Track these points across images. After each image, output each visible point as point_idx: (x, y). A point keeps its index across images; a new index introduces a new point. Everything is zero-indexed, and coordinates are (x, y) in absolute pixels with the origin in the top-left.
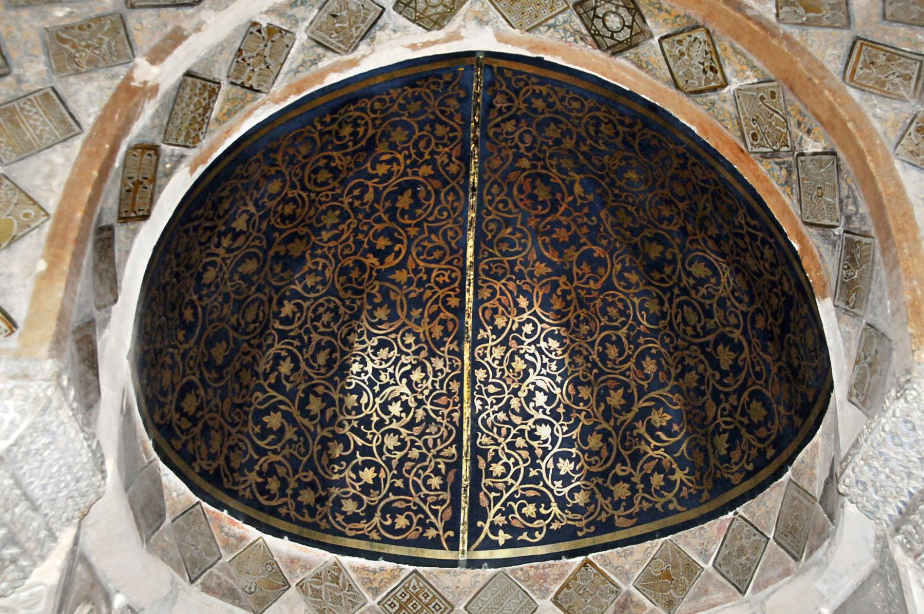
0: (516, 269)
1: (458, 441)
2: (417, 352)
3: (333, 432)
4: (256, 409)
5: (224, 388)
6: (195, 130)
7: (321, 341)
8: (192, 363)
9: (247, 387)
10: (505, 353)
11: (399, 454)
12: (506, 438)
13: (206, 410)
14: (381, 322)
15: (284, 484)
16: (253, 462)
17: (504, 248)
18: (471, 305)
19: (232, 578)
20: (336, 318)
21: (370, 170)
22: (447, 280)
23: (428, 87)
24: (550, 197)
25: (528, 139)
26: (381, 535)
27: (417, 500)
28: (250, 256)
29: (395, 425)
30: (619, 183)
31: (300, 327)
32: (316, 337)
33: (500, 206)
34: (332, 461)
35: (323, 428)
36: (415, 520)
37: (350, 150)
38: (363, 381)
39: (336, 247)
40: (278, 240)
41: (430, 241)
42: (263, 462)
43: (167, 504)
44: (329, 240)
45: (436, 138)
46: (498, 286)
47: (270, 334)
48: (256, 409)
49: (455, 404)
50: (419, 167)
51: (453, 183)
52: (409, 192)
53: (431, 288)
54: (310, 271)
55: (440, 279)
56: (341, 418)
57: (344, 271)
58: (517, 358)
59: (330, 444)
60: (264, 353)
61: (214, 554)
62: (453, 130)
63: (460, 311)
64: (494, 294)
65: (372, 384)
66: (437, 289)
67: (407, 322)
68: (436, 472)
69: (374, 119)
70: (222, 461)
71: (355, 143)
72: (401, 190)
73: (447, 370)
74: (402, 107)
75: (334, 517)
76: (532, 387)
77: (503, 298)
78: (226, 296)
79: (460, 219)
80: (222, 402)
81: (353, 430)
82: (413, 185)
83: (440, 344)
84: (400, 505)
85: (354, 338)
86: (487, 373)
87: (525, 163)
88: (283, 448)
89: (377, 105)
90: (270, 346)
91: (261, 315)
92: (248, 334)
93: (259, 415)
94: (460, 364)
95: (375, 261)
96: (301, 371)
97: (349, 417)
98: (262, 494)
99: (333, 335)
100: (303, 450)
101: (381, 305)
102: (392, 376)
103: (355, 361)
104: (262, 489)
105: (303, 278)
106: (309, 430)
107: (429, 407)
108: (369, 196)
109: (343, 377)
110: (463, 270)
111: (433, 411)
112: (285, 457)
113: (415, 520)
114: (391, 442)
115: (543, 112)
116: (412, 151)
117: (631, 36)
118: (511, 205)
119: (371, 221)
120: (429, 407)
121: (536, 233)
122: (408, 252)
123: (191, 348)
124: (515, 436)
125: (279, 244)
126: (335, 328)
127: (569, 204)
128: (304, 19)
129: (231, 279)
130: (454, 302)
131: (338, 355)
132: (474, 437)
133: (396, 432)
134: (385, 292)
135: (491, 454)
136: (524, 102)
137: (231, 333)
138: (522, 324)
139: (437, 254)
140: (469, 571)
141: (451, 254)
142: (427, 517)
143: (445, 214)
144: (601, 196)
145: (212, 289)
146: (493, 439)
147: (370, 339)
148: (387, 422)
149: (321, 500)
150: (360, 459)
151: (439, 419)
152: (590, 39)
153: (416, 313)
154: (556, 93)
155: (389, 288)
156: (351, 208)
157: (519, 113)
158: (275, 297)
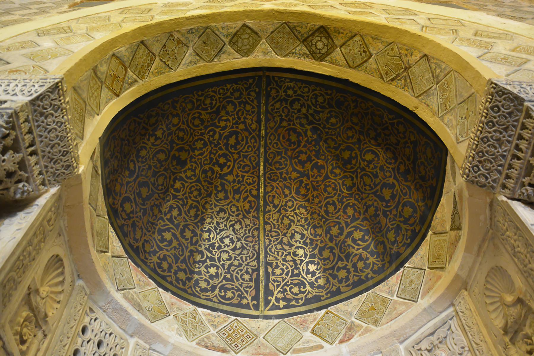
0: (283, 176)
4: (159, 228)
5: (145, 210)
7: (192, 204)
8: (131, 189)
9: (156, 216)
10: (280, 216)
13: (135, 216)
14: (221, 200)
17: (277, 166)
18: (263, 195)
20: (200, 194)
21: (217, 124)
22: (252, 182)
23: (243, 85)
24: (297, 139)
25: (286, 110)
28: (163, 151)
30: (327, 126)
31: (183, 195)
32: (190, 202)
33: (275, 145)
35: (191, 245)
37: (209, 111)
38: (211, 227)
39: (201, 159)
40: (175, 149)
41: (244, 162)
42: (161, 254)
43: (110, 246)
44: (199, 155)
45: (247, 111)
46: (275, 184)
47: (169, 195)
48: (159, 228)
49: (256, 242)
50: (239, 124)
51: (254, 134)
52: (234, 137)
53: (244, 185)
54: (189, 169)
55: (248, 181)
56: (200, 242)
57: (205, 172)
58: (285, 218)
59: (194, 254)
60: (165, 203)
61: (132, 284)
62: (253, 108)
63: (257, 197)
64: (273, 189)
65: (216, 229)
66: (247, 185)
67: (233, 200)
69: (220, 98)
70: (140, 244)
71: (212, 108)
72: (231, 134)
73: (252, 225)
74: (232, 94)
77: (278, 190)
78: (150, 167)
79: (257, 152)
80: (144, 216)
82: (236, 133)
83: (248, 212)
85: (207, 206)
86: (271, 227)
87: (284, 124)
89: (221, 91)
90: (169, 201)
91: (165, 185)
92: (158, 190)
93: (160, 232)
94: (258, 222)
96: (182, 216)
99: (198, 202)
100: (181, 253)
101: (221, 191)
102: (226, 226)
103: (208, 218)
105: (185, 172)
106: (184, 244)
107: (243, 242)
108: (217, 136)
110: (259, 177)
111: (245, 244)
112: (172, 254)
115: (292, 97)
116: (236, 116)
117: (328, 49)
118: (279, 145)
119: (217, 149)
120: (243, 242)
121: (291, 158)
122: (234, 166)
125: (176, 150)
126: (199, 199)
127: (306, 142)
129: (153, 159)
130: (255, 192)
131: (200, 213)
134: (222, 185)
136: (284, 92)
137: (151, 186)
138: (287, 202)
139: (247, 169)
141: (253, 169)
143: (250, 148)
144: (320, 134)
147: (215, 207)
148: (223, 247)
152: (310, 56)
153: (237, 197)
154: (297, 85)
155: (224, 184)
156: (209, 141)
157: (282, 98)
158: (172, 177)
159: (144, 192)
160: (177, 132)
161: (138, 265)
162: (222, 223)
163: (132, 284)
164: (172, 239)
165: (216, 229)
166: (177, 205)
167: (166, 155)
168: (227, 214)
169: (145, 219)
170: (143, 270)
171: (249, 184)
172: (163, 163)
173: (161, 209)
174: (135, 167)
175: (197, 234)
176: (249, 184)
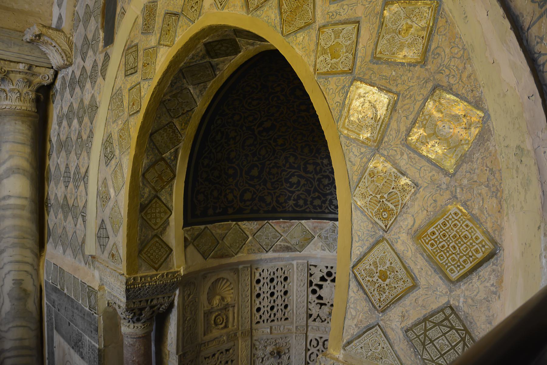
3: (322, 175)
15: (305, 201)
19: (288, 242)
35: (317, 175)
43: (248, 233)
59: (322, 180)
88: (301, 188)
93: (287, 181)
98: (296, 207)
100: (310, 186)
106: (311, 178)
112: (303, 191)
128: (183, 84)
149: (324, 202)
159: (255, 172)
161: (278, 218)
169: (269, 185)
170: (284, 219)
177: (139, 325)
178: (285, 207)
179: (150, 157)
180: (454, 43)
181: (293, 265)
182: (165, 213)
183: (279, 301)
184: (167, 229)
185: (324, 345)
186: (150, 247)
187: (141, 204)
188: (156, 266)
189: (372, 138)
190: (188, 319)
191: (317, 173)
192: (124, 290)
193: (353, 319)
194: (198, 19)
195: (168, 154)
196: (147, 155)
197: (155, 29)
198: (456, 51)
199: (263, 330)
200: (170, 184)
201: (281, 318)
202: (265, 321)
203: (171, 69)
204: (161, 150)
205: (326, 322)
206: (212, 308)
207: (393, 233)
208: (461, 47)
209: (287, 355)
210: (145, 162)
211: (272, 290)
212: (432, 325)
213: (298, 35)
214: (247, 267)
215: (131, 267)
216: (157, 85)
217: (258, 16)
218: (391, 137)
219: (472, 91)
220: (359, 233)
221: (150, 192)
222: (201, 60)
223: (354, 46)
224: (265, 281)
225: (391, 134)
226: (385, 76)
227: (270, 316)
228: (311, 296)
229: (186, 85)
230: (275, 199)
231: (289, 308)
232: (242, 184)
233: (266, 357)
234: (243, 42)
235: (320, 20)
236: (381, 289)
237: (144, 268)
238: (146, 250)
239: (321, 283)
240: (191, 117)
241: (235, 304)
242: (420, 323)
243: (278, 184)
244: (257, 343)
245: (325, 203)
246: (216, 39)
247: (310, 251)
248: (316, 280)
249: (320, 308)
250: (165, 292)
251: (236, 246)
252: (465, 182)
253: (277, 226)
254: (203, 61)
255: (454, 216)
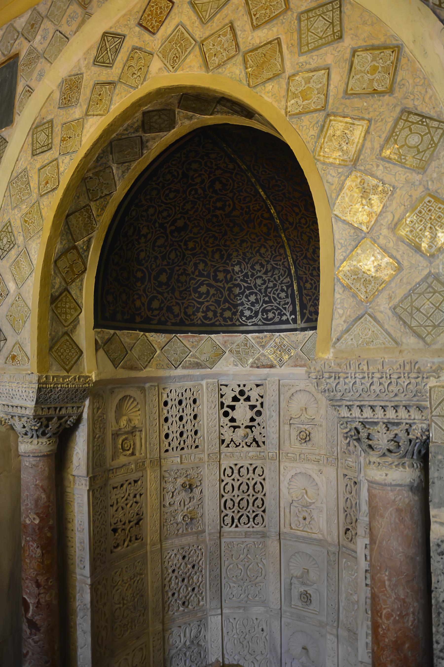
1: (290, 274)
2: (259, 241)
3: (232, 284)
6: (89, 227)
7: (213, 250)
9: (186, 281)
11: (264, 286)
12: (309, 271)
15: (215, 313)
16: (198, 309)
19: (198, 358)
22: (259, 208)
26: (263, 322)
27: (276, 305)
29: (259, 274)
31: (201, 249)
32: (210, 250)
33: (263, 173)
34: (236, 296)
36: (277, 314)
42: (203, 307)
48: (193, 288)
49: (284, 259)
52: (217, 183)
53: (253, 213)
55: (255, 208)
58: (303, 235)
59: (233, 289)
60: (189, 265)
61: (187, 352)
68: (282, 290)
70: (182, 315)
73: (276, 244)
75: (242, 319)
76: (313, 247)
81: (241, 280)
84: (269, 308)
85: (228, 243)
88: (210, 298)
89: (174, 163)
91: (179, 254)
93: (195, 290)
95: (221, 212)
97: (238, 276)
98: (206, 320)
99: (218, 245)
100: (220, 296)
102: (252, 253)
104: (205, 318)
106: (221, 287)
108: (200, 191)
109: (230, 260)
112: (212, 302)
113: (277, 314)
114: (259, 282)
116: (207, 168)
120: (272, 263)
123: (146, 286)
124: (312, 270)
125: (170, 226)
128: (108, 161)
129: (154, 250)
131: (224, 252)
132: (296, 272)
133: (260, 277)
135: (304, 279)
137: (166, 267)
138: (300, 219)
139: (248, 199)
140: (303, 333)
142: (282, 311)
143: (241, 184)
145: (146, 259)
146: (304, 272)
149: (234, 314)
150: (248, 292)
151: (278, 267)
158: (182, 244)
159: (163, 278)
160: (160, 216)
161: (186, 332)
162: (248, 252)
163: (187, 352)
164: (208, 289)
165: (244, 259)
166: (199, 260)
167: (163, 237)
168: (249, 243)
169: (177, 294)
170: (192, 332)
171: (258, 210)
172: (166, 244)
173: (187, 272)
174: (143, 272)
175: (229, 271)
176: (258, 210)
177: (44, 440)
178: (193, 320)
179: (64, 242)
180: (416, 75)
181: (202, 385)
182: (76, 310)
183: (189, 426)
184: (77, 328)
185: (239, 472)
186: (60, 345)
187: (52, 295)
188: (67, 368)
189: (348, 159)
190: (97, 436)
191: (227, 282)
192: (35, 391)
193: (341, 317)
194: (142, 84)
195: (80, 242)
196: (61, 239)
197: (80, 101)
198: (418, 81)
199: (172, 459)
200: (81, 278)
201: (192, 446)
202: (175, 449)
203: (102, 140)
204: (74, 236)
205: (241, 446)
206: (120, 429)
207: (374, 231)
208: (421, 77)
209: (199, 488)
210: (58, 247)
211: (181, 414)
212: (417, 296)
213: (267, 85)
214: (155, 386)
215: (42, 365)
216: (84, 157)
217: (219, 73)
218: (366, 155)
219: (434, 108)
220: (342, 241)
221: (61, 283)
222: (134, 133)
223: (325, 88)
224: (173, 402)
225: (367, 151)
226: (358, 107)
227: (179, 444)
228: (223, 418)
229: (110, 163)
230: (183, 310)
231: (199, 434)
232: (150, 290)
233: (177, 491)
234: (182, 114)
235: (289, 70)
236: (367, 282)
237: (54, 368)
238: (56, 347)
239: (233, 403)
240: (108, 203)
241: (142, 427)
242: (406, 298)
243: (186, 294)
244: (167, 475)
245: (235, 315)
246: (158, 107)
247: (221, 368)
248: (228, 401)
249: (234, 432)
250: (74, 400)
251: (144, 358)
252: (435, 175)
253: (186, 340)
254: (135, 135)
255: (428, 203)
